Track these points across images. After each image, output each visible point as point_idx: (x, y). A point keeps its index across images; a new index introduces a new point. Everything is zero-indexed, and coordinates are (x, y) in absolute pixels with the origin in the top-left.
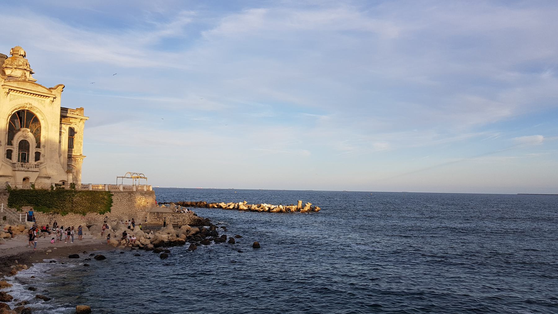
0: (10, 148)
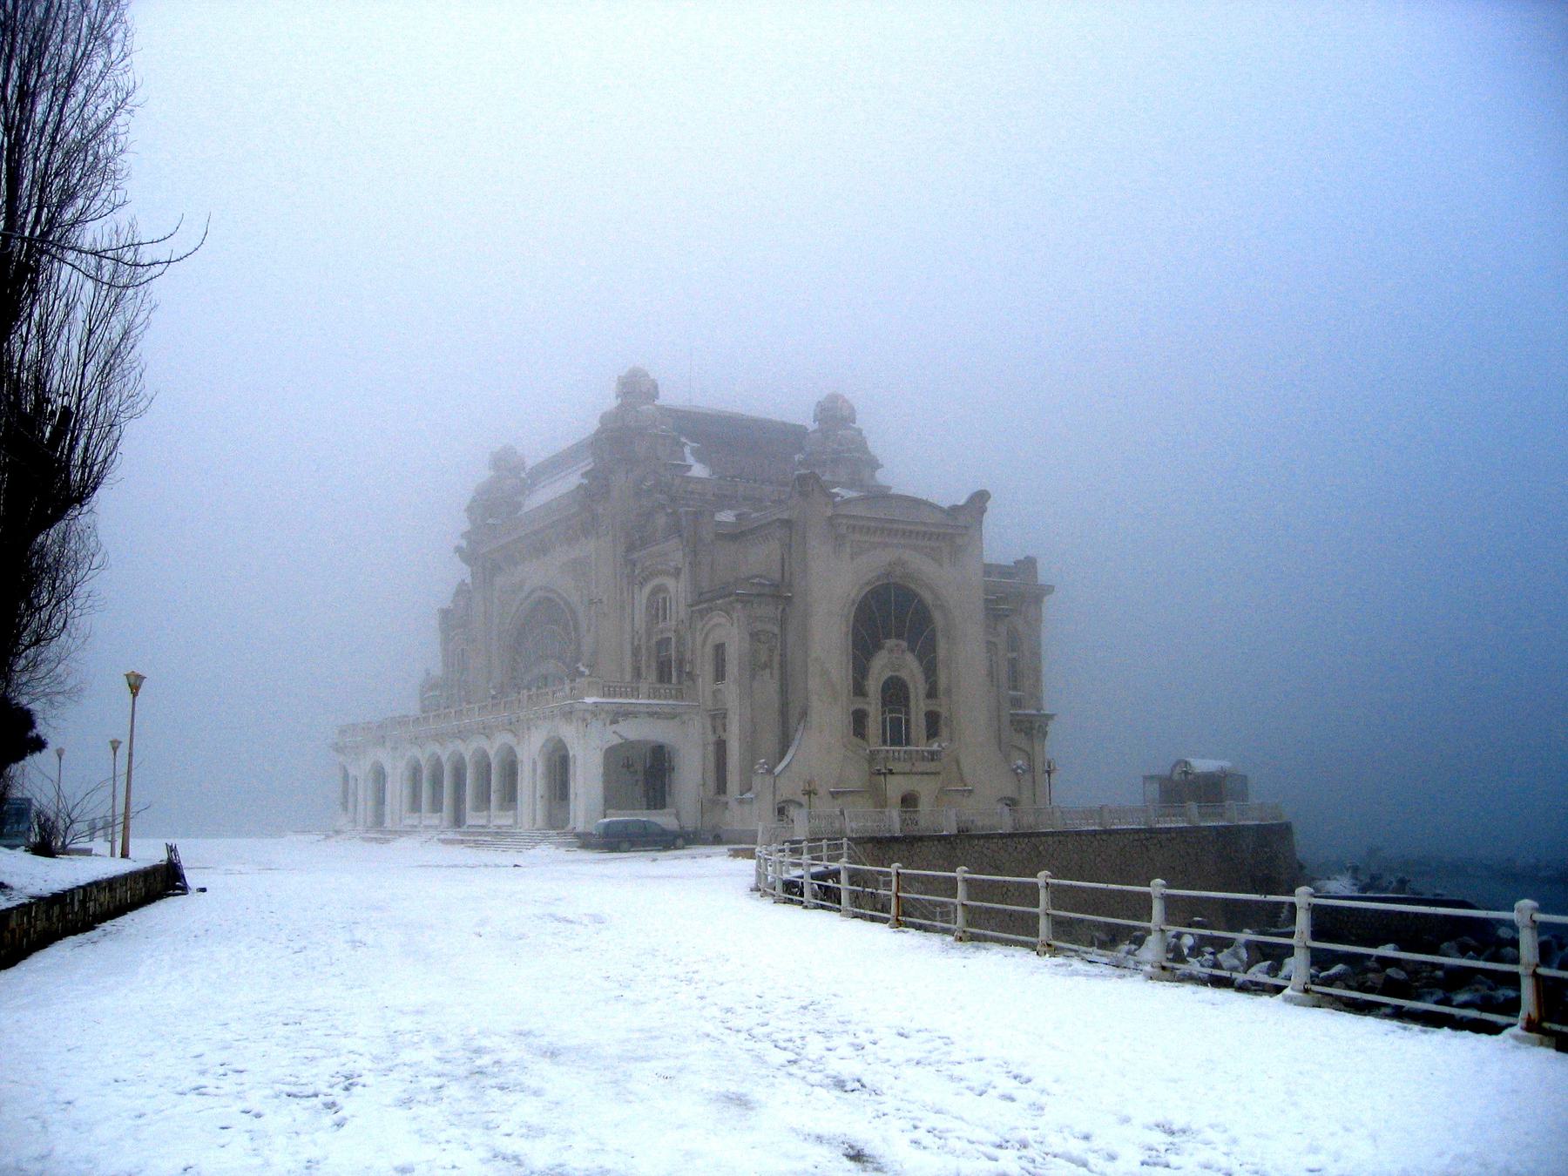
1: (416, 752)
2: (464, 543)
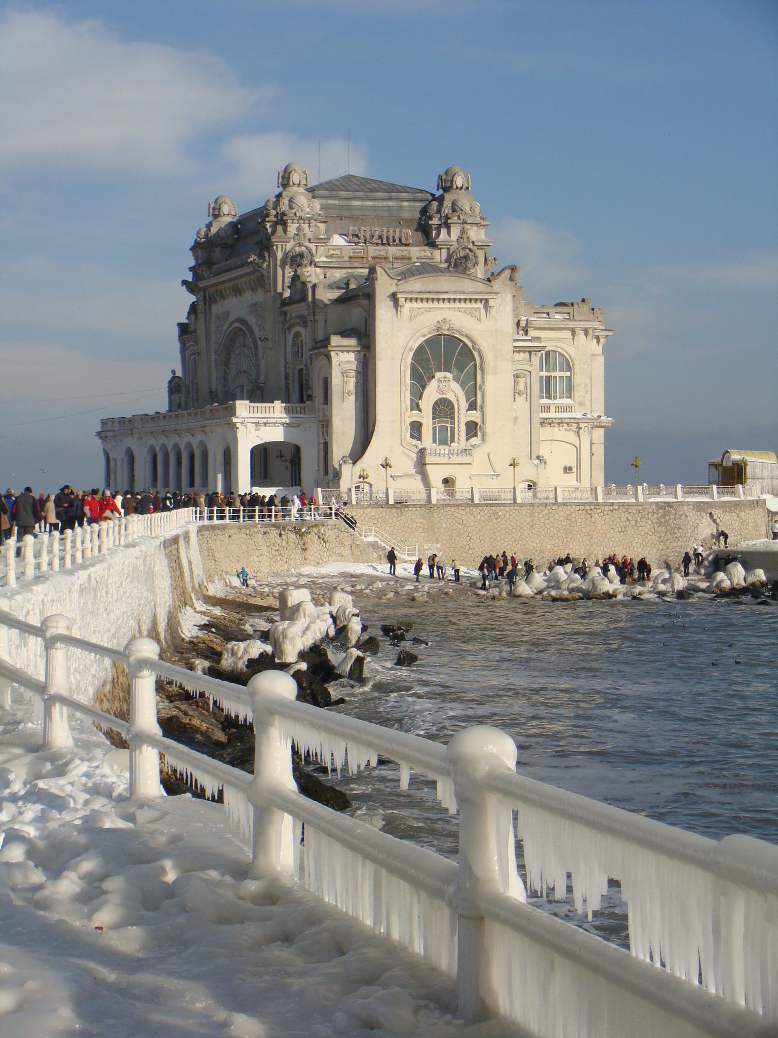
0: (415, 416)
1: (152, 442)
2: (189, 277)
